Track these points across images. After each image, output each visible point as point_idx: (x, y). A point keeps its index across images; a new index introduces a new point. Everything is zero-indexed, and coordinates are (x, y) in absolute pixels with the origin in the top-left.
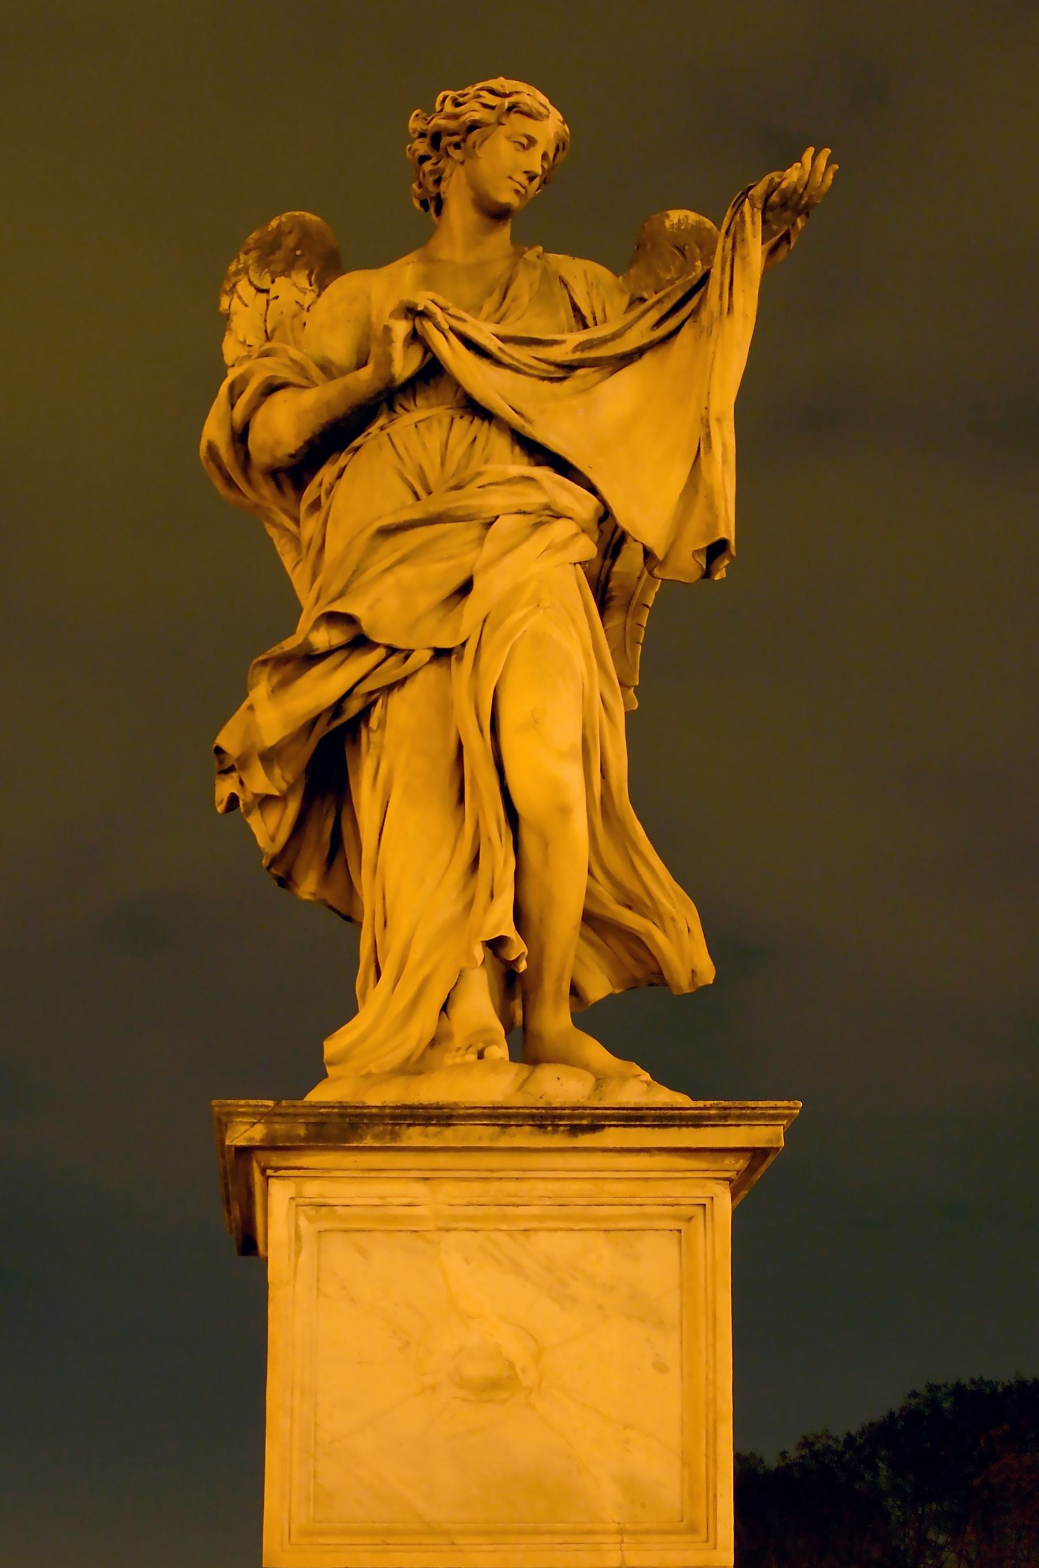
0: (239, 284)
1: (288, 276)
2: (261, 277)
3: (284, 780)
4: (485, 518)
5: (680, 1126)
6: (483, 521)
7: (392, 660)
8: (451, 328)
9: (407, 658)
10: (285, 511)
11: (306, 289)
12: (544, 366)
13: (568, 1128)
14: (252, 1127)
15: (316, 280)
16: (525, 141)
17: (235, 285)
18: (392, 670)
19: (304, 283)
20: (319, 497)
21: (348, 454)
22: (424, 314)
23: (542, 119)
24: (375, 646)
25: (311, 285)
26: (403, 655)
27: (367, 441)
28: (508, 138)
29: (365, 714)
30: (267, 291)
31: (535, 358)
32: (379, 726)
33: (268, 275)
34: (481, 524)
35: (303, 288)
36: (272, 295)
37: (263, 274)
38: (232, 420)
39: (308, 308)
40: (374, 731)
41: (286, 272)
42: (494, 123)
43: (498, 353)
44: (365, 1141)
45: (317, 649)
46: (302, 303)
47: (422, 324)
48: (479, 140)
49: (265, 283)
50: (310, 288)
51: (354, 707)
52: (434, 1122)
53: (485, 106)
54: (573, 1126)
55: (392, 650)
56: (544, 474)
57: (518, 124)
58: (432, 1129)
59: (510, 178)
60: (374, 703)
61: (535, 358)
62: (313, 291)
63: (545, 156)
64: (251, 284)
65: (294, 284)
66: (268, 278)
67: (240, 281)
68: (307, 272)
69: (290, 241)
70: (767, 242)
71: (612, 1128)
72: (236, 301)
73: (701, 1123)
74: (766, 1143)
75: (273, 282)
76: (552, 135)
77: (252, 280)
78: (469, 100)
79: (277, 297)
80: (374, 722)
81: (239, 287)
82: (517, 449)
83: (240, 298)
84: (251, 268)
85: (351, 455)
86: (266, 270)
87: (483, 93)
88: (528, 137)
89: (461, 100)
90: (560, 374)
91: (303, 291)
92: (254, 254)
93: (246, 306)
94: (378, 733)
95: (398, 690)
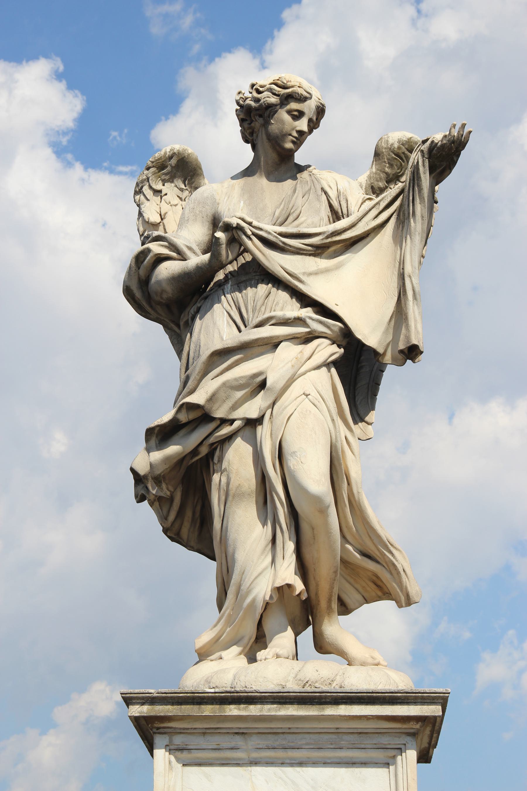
0: (144, 187)
1: (172, 182)
2: (156, 183)
3: (168, 489)
4: (275, 343)
6: (273, 344)
8: (254, 234)
9: (231, 424)
10: (173, 322)
11: (183, 189)
12: (310, 248)
15: (188, 184)
16: (296, 113)
17: (142, 187)
19: (183, 186)
20: (188, 320)
21: (201, 300)
22: (239, 228)
24: (213, 419)
25: (185, 186)
26: (230, 422)
27: (211, 294)
28: (289, 112)
29: (211, 455)
30: (160, 191)
31: (303, 244)
32: (219, 461)
33: (160, 181)
34: (272, 345)
35: (181, 188)
36: (163, 193)
37: (157, 181)
38: (139, 274)
39: (185, 199)
40: (216, 464)
41: (171, 180)
45: (182, 421)
46: (181, 197)
47: (237, 233)
49: (158, 186)
50: (185, 188)
51: (204, 450)
53: (274, 94)
56: (307, 313)
58: (242, 706)
59: (290, 135)
60: (215, 449)
61: (303, 244)
62: (187, 189)
63: (310, 120)
64: (150, 187)
65: (176, 186)
66: (160, 183)
68: (183, 179)
69: (173, 162)
70: (433, 173)
72: (142, 197)
75: (164, 185)
76: (314, 107)
77: (151, 185)
78: (265, 91)
79: (166, 194)
80: (216, 459)
81: (144, 189)
83: (144, 195)
84: (150, 178)
85: (203, 301)
87: (274, 86)
89: (261, 89)
91: (182, 190)
92: (152, 170)
93: (148, 200)
94: (218, 465)
95: (229, 441)
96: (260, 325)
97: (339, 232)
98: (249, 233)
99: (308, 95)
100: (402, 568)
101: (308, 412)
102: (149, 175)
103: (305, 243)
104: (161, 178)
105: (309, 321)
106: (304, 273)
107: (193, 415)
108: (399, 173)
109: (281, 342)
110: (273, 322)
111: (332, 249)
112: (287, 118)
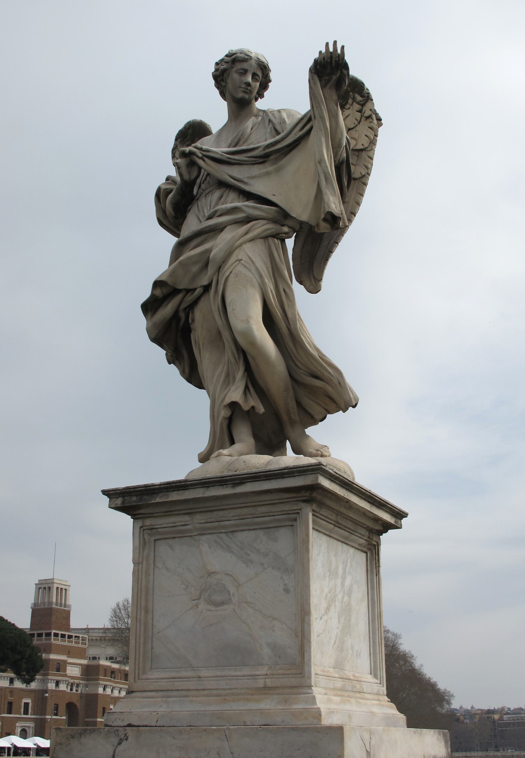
5: (276, 478)
7: (189, 294)
9: (194, 292)
12: (252, 159)
13: (232, 485)
14: (118, 499)
18: (190, 298)
23: (256, 59)
26: (193, 291)
28: (236, 72)
42: (230, 68)
43: (228, 160)
44: (156, 500)
48: (227, 76)
52: (181, 489)
54: (234, 484)
55: (188, 291)
57: (238, 66)
59: (240, 87)
67: (176, 152)
71: (249, 483)
73: (284, 476)
74: (311, 482)
82: (241, 196)
84: (178, 146)
86: (185, 145)
88: (243, 69)
90: (262, 160)
96: (210, 218)
97: (273, 144)
98: (200, 155)
99: (249, 58)
100: (338, 381)
101: (240, 272)
102: (178, 144)
103: (248, 156)
104: (186, 144)
105: (244, 208)
106: (248, 178)
107: (165, 291)
108: (343, 102)
109: (226, 227)
110: (217, 214)
111: (272, 157)
112: (236, 76)
